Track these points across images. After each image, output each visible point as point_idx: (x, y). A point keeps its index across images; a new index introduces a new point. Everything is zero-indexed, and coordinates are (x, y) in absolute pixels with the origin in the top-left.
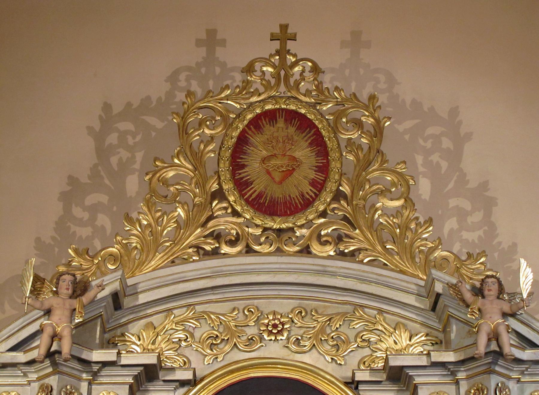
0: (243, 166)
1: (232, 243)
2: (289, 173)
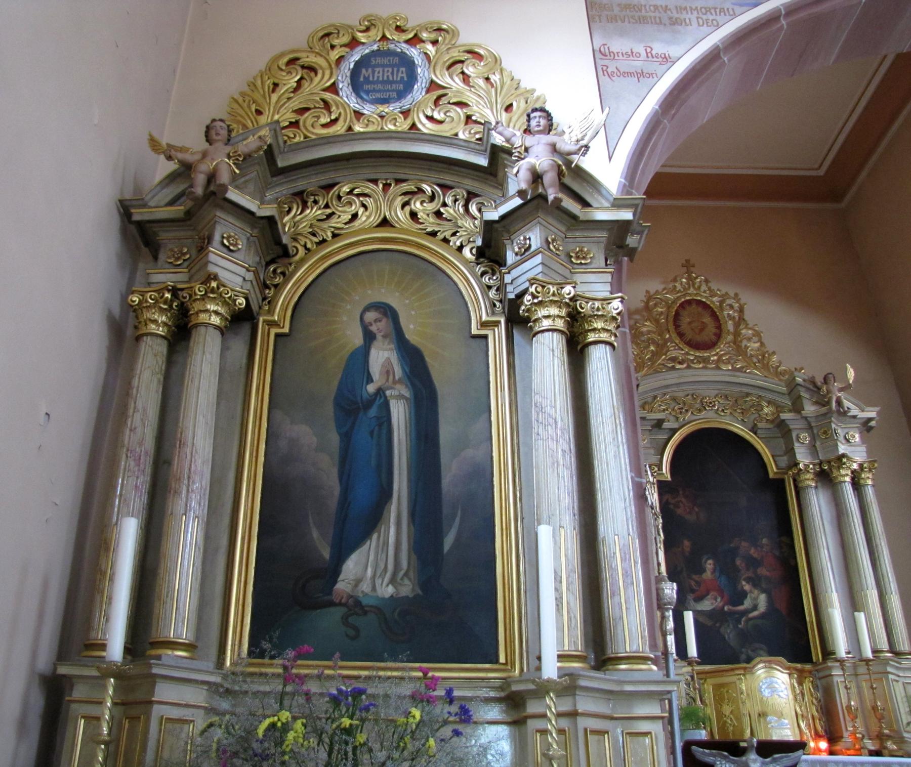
0: (679, 326)
1: (680, 363)
2: (702, 330)
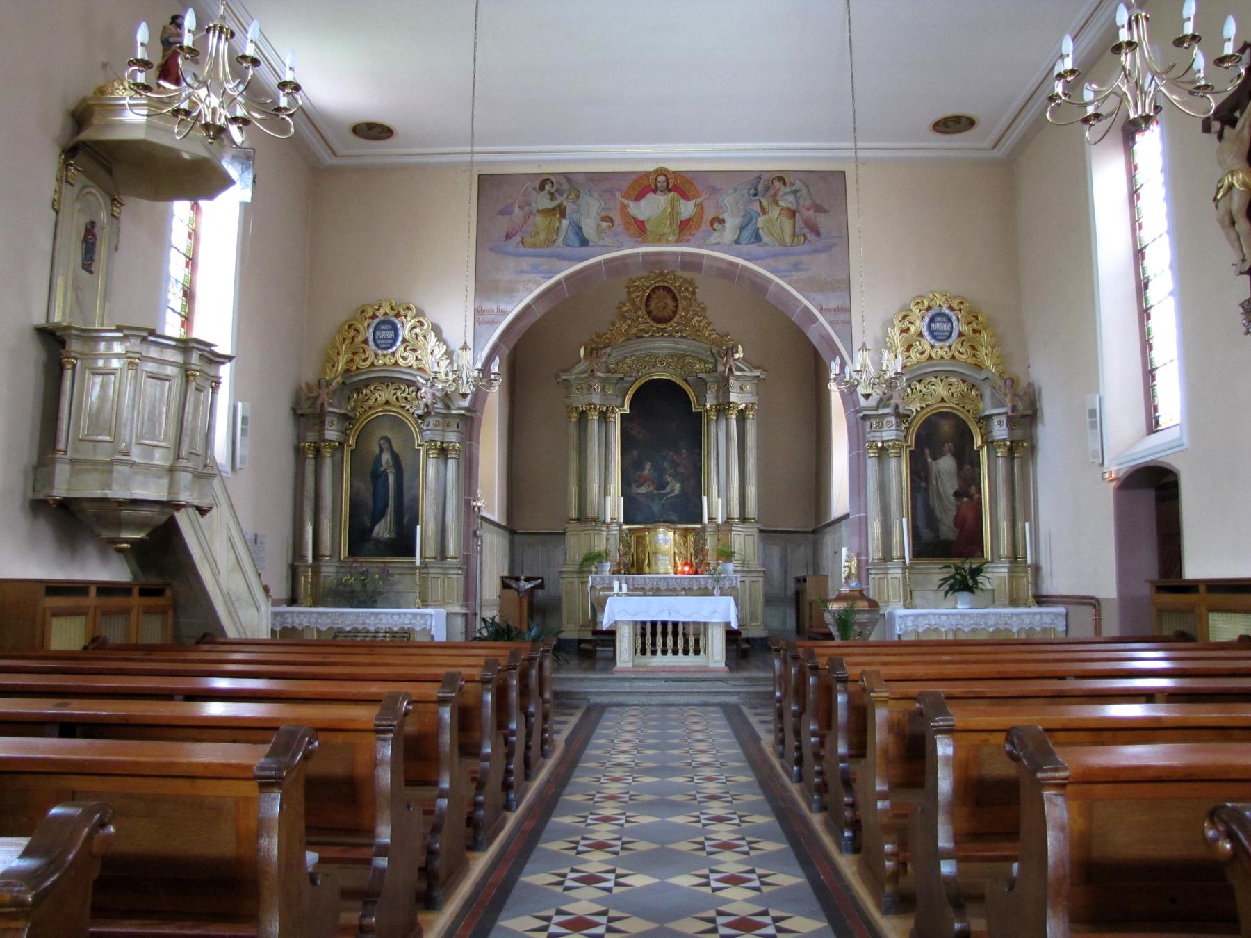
2: (665, 308)
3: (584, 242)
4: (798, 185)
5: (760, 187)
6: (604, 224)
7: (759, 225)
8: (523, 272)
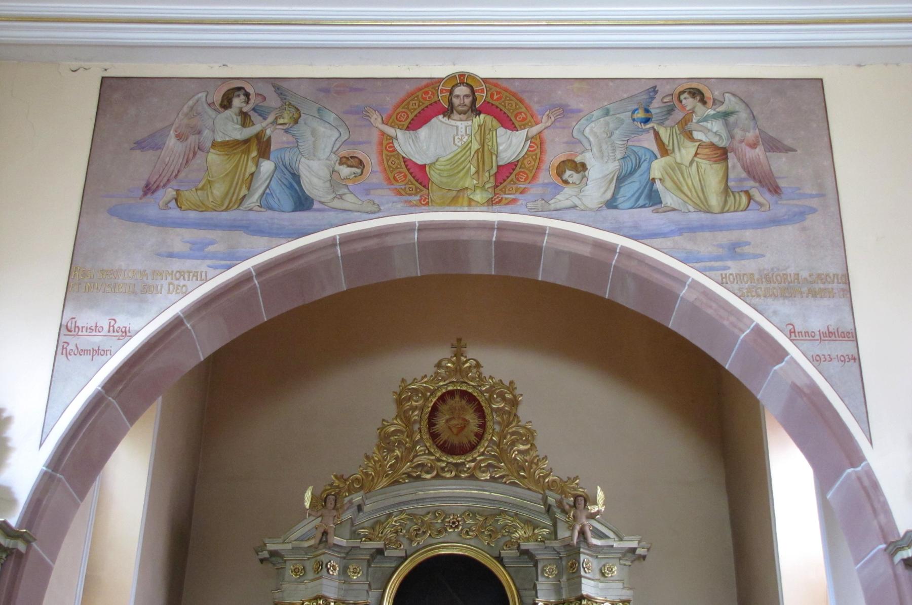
0: (435, 425)
2: (462, 429)
3: (303, 202)
4: (731, 102)
5: (656, 107)
6: (345, 171)
7: (656, 173)
8: (171, 255)
